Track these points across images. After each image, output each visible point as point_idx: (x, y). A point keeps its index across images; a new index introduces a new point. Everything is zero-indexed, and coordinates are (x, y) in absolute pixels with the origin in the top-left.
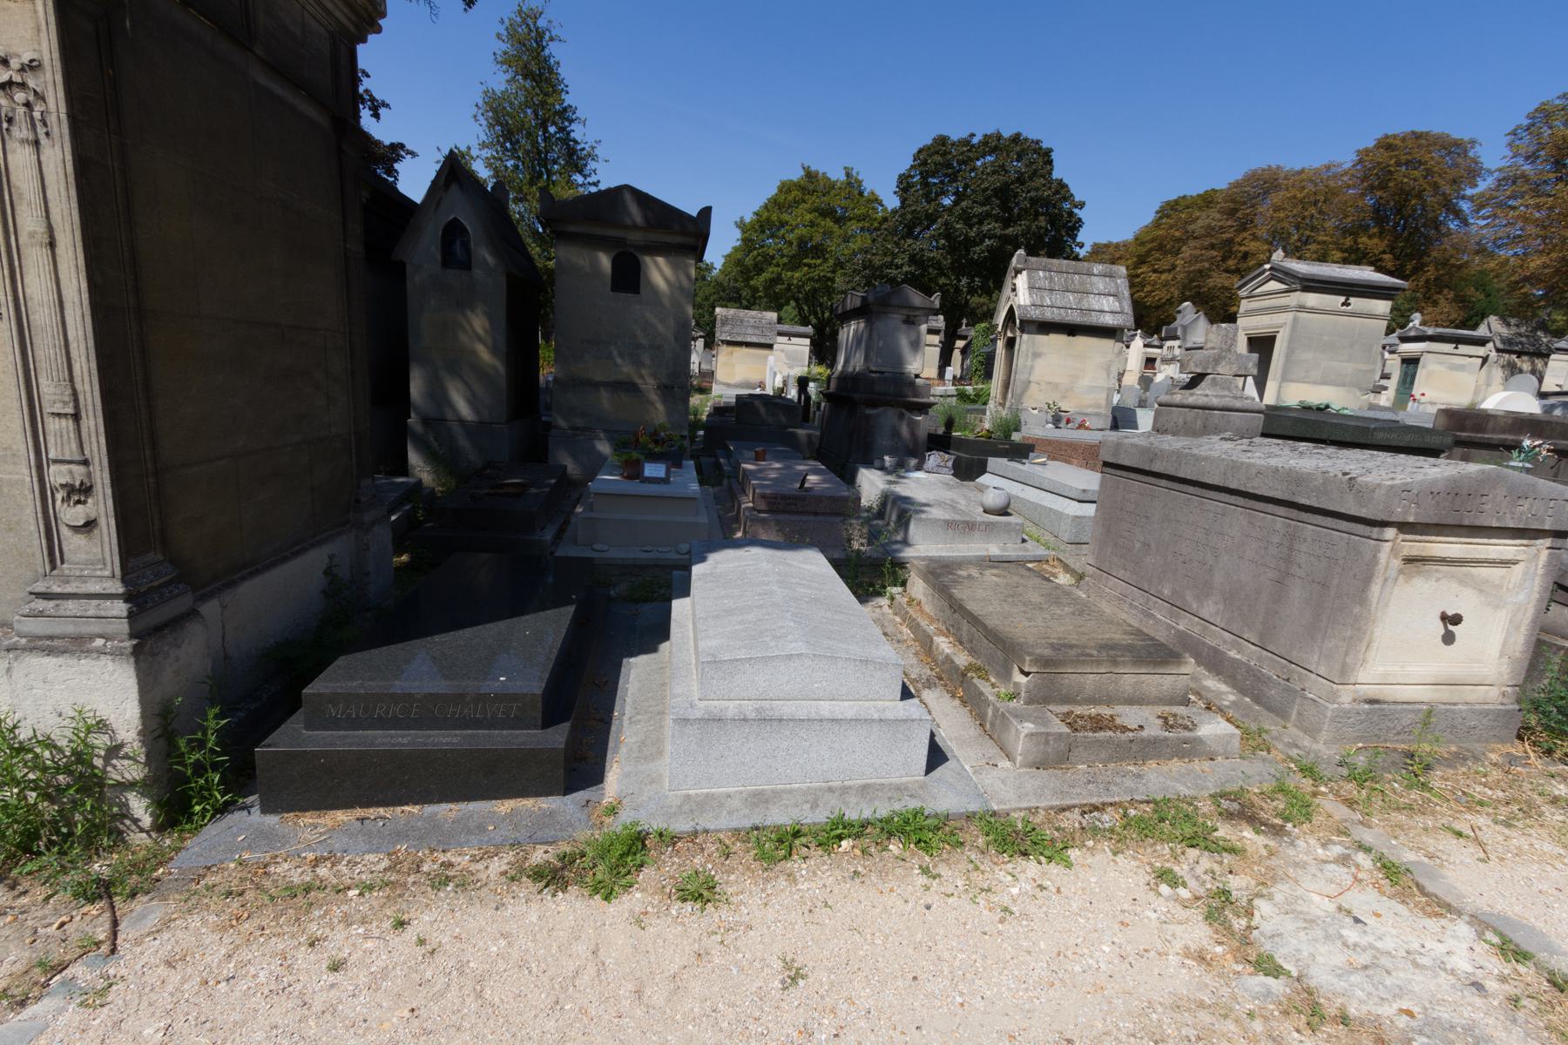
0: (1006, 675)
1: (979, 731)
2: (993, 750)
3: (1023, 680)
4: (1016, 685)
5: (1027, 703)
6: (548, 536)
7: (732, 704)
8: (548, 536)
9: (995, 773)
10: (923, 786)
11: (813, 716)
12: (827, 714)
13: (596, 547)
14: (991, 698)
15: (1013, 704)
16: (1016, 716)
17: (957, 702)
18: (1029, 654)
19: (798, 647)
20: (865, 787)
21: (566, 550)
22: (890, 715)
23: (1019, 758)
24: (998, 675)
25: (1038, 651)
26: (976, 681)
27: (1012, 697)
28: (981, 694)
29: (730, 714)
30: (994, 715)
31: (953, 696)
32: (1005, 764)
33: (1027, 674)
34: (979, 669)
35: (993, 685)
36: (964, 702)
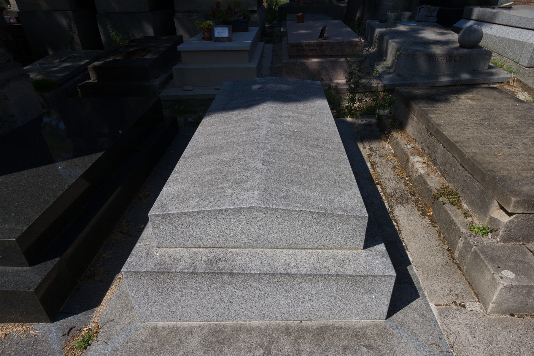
0: (483, 208)
1: (447, 257)
2: (462, 286)
3: (505, 219)
4: (493, 220)
5: (505, 240)
6: (157, 83)
7: (186, 253)
8: (157, 83)
9: (462, 317)
10: (383, 333)
11: (266, 269)
12: (280, 267)
13: (186, 88)
14: (463, 230)
15: (488, 240)
16: (492, 259)
17: (426, 221)
18: (516, 193)
19: (250, 197)
20: (323, 330)
21: (169, 92)
22: (349, 270)
23: (491, 306)
24: (471, 203)
25: (525, 189)
26: (447, 207)
27: (485, 232)
28: (452, 222)
29: (180, 267)
30: (464, 247)
31: (423, 214)
32: (473, 305)
33: (510, 214)
34: (450, 194)
35: (466, 214)
36: (433, 222)
